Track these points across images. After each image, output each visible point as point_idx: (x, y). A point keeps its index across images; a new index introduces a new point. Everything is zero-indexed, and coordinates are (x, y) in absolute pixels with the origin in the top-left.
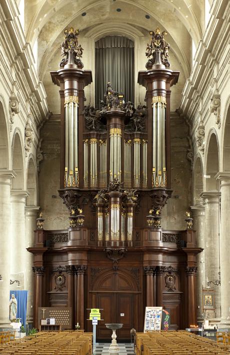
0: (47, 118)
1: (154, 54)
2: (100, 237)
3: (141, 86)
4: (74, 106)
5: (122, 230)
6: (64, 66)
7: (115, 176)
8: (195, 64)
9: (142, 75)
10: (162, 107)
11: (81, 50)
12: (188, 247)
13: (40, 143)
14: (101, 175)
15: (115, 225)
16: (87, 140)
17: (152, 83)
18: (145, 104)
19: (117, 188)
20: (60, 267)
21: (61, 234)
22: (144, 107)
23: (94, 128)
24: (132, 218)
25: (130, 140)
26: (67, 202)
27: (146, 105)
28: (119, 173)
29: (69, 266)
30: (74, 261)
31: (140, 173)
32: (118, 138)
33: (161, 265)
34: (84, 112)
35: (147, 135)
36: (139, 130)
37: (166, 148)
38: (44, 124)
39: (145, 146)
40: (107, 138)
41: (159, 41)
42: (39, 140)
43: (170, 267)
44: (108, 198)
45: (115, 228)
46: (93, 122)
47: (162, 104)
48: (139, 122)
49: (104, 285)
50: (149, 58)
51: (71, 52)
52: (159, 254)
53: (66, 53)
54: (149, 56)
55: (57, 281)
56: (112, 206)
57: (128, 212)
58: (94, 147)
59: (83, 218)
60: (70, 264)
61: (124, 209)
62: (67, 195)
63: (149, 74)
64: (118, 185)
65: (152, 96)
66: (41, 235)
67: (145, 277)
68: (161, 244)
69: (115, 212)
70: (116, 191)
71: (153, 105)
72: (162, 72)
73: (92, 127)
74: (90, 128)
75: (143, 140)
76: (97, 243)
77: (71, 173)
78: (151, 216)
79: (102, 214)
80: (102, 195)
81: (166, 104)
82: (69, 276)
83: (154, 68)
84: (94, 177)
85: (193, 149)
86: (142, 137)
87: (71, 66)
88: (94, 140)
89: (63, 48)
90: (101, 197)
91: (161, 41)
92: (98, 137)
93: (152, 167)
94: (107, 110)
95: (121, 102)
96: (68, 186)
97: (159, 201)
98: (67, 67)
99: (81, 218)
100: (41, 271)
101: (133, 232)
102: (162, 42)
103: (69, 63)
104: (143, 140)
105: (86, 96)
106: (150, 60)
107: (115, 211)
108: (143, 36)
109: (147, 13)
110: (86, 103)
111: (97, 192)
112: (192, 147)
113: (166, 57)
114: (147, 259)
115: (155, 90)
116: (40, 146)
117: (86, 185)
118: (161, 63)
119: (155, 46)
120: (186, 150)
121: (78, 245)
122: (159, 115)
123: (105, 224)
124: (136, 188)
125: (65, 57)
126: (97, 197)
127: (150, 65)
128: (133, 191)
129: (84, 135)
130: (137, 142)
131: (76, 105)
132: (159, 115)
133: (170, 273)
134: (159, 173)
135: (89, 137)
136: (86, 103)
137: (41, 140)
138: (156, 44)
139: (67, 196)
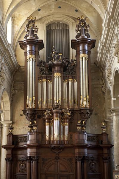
0: (17, 69)
1: (80, 30)
2: (47, 138)
3: (73, 49)
4: (32, 61)
5: (61, 133)
6: (27, 38)
10: (86, 60)
11: (37, 29)
12: (103, 144)
13: (13, 83)
14: (49, 101)
15: (56, 130)
16: (40, 80)
17: (79, 46)
18: (75, 58)
20: (23, 158)
21: (23, 137)
22: (75, 60)
23: (44, 73)
25: (67, 80)
26: (28, 118)
27: (76, 60)
28: (59, 99)
29: (28, 157)
32: (59, 78)
33: (86, 156)
34: (39, 64)
36: (72, 74)
37: (88, 84)
38: (16, 72)
39: (76, 83)
40: (52, 79)
41: (83, 23)
42: (12, 82)
43: (92, 157)
44: (52, 114)
45: (56, 133)
46: (44, 70)
47: (86, 58)
48: (72, 69)
49: (50, 169)
51: (31, 30)
52: (85, 149)
53: (28, 31)
55: (20, 167)
56: (55, 118)
58: (44, 84)
59: (36, 126)
60: (28, 155)
61: (62, 121)
62: (28, 113)
63: (77, 41)
64: (58, 106)
65: (79, 54)
66: (11, 137)
67: (76, 163)
68: (86, 142)
69: (57, 122)
71: (80, 59)
72: (85, 40)
75: (75, 80)
77: (31, 99)
78: (79, 124)
79: (48, 124)
81: (88, 58)
82: (28, 163)
84: (44, 102)
85: (105, 85)
86: (73, 78)
87: (31, 37)
88: (44, 80)
89: (26, 28)
90: (48, 113)
93: (80, 96)
96: (28, 107)
97: (85, 116)
98: (28, 38)
99: (35, 126)
100: (10, 160)
101: (68, 135)
102: (85, 24)
103: (30, 36)
104: (75, 80)
106: (78, 34)
107: (57, 122)
108: (74, 22)
109: (76, 8)
111: (45, 111)
112: (104, 84)
113: (87, 32)
114: (78, 152)
115: (81, 50)
116: (13, 85)
117: (40, 107)
118: (84, 35)
119: (81, 26)
120: (101, 87)
121: (34, 143)
122: (83, 65)
125: (28, 33)
126: (45, 113)
127: (78, 36)
129: (38, 79)
131: (34, 60)
132: (83, 65)
133: (92, 161)
134: (85, 99)
135: (42, 78)
136: (40, 59)
137: (14, 82)
138: (81, 24)
139: (28, 114)
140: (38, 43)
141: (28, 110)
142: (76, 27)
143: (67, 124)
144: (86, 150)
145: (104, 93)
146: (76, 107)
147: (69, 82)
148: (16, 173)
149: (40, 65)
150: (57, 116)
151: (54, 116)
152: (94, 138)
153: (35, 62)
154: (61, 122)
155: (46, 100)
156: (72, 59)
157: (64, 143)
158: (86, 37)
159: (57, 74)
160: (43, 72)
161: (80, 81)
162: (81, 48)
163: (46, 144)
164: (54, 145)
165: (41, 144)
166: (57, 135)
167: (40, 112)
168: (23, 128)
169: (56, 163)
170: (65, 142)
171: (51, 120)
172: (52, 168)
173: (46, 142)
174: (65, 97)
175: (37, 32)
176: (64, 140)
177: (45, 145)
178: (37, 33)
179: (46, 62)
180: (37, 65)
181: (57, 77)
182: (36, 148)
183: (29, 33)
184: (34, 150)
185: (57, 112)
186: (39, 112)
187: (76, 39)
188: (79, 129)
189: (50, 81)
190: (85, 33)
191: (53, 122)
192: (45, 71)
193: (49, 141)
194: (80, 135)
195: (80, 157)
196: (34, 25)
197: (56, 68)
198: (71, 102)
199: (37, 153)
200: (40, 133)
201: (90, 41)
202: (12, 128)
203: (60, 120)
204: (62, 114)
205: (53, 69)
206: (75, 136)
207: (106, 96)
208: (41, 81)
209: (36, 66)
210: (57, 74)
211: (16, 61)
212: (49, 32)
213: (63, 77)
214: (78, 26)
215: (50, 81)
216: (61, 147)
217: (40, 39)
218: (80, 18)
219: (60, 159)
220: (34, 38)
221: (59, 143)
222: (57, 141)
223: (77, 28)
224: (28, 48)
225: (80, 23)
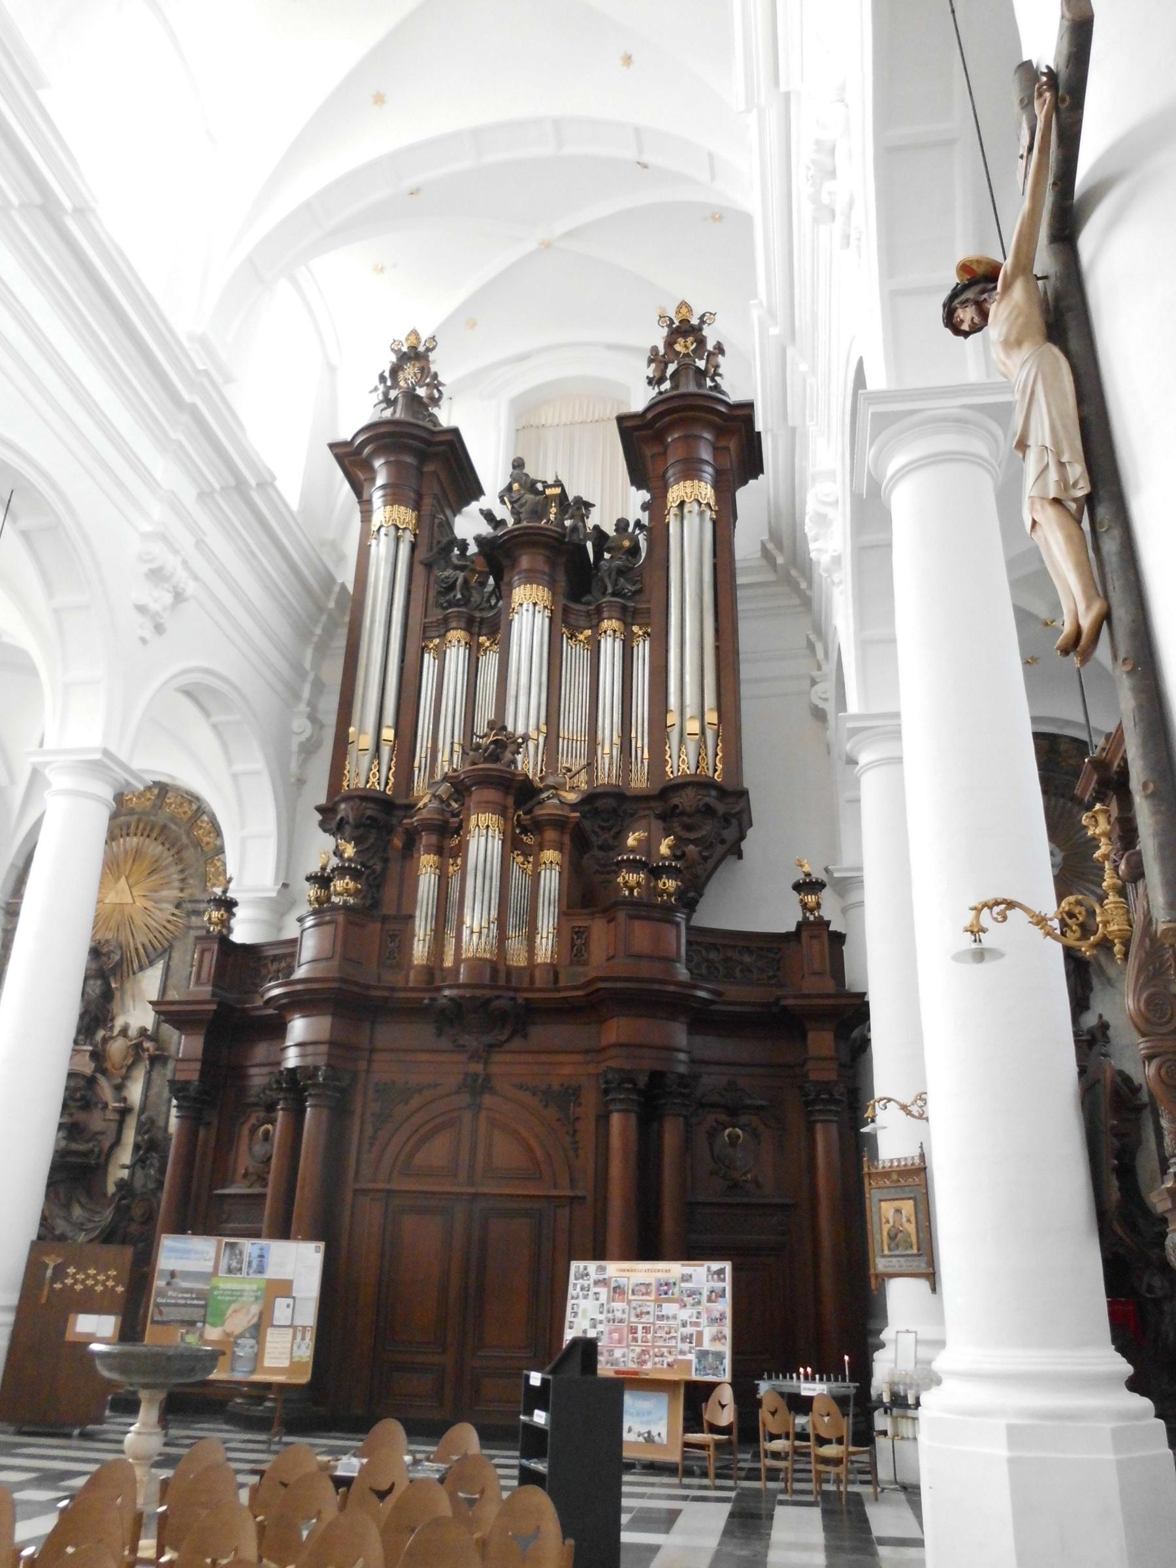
2: (420, 951)
18: (645, 518)
25: (588, 632)
33: (682, 1069)
35: (648, 610)
37: (717, 648)
39: (643, 650)
47: (700, 504)
49: (419, 1159)
58: (456, 657)
60: (292, 1059)
67: (603, 1119)
69: (484, 841)
75: (635, 629)
76: (408, 976)
86: (628, 616)
90: (439, 798)
92: (473, 626)
100: (184, 1098)
102: (701, 342)
104: (635, 629)
134: (693, 726)
135: (444, 626)
138: (678, 347)
147: (599, 641)
148: (223, 1187)
150: (485, 807)
152: (747, 959)
153: (414, 547)
154: (512, 844)
157: (526, 979)
166: (476, 929)
169: (467, 1117)
171: (448, 835)
172: (437, 1152)
173: (412, 974)
180: (421, 563)
181: (529, 614)
188: (631, 890)
191: (461, 850)
197: (525, 562)
201: (723, 409)
209: (419, 569)
211: (305, 543)
215: (488, 644)
218: (671, 319)
219: (492, 1090)
221: (487, 980)
222: (477, 963)
223: (653, 365)
225: (670, 344)
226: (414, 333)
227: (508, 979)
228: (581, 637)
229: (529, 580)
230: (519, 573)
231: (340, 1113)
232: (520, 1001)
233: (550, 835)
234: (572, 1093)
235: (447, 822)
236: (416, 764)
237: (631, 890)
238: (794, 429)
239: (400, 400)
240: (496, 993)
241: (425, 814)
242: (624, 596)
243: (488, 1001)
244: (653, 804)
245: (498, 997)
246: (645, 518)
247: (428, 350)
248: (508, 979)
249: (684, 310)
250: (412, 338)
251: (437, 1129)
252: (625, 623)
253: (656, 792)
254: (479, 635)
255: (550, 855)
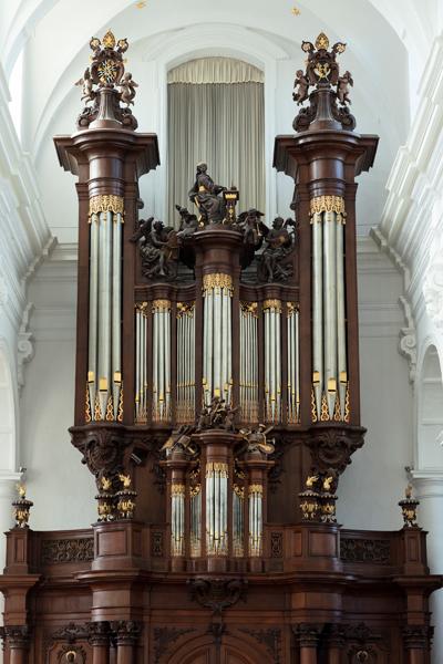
0: (46, 252)
1: (313, 97)
2: (177, 546)
4: (112, 221)
5: (234, 529)
6: (87, 125)
7: (217, 393)
8: (416, 119)
9: (283, 144)
10: (336, 222)
11: (132, 86)
12: (407, 573)
13: (26, 313)
14: (180, 392)
15: (214, 516)
16: (145, 304)
17: (309, 164)
18: (292, 215)
19: (220, 421)
20: (72, 626)
21: (76, 541)
22: (290, 222)
23: (162, 273)
24: (260, 499)
25: (255, 305)
26: (92, 460)
27: (294, 220)
28: (225, 386)
29: (96, 623)
30: (109, 611)
31: (282, 387)
32: (225, 298)
33: (338, 621)
34: (137, 232)
35: (298, 291)
36: (277, 278)
38: (36, 268)
39: (294, 320)
41: (326, 65)
42: (23, 307)
43: (361, 626)
44: (198, 446)
45: (216, 529)
46: (161, 259)
48: (278, 260)
50: (301, 107)
51: (107, 93)
52: (332, 592)
53: (94, 95)
54: (301, 102)
56: (209, 467)
57: (250, 483)
58: (162, 320)
59: (132, 498)
60: (98, 616)
61: (240, 476)
62: (93, 441)
63: (301, 142)
64: (224, 414)
65: (310, 196)
66: (23, 543)
68: (337, 566)
69: (216, 482)
70: (220, 433)
71: (312, 217)
72: (334, 138)
73: (159, 271)
74: (153, 274)
75: (289, 305)
76: (170, 562)
77: (104, 384)
78: (309, 493)
79: (180, 487)
80: (183, 439)
81: (345, 214)
83: (314, 127)
84: (161, 397)
85: (416, 326)
86: (284, 296)
87: (107, 123)
88: (162, 304)
89: (86, 83)
90: (181, 446)
91: (330, 67)
92: (172, 296)
93: (312, 371)
94: (196, 231)
95: (231, 211)
96: (94, 418)
97: (330, 456)
98: (94, 126)
99: (126, 497)
101: (263, 534)
102: (334, 69)
103: (101, 118)
104: (289, 305)
105: (142, 196)
106: (303, 111)
108: (285, 59)
110: (143, 215)
111: (167, 433)
112: (411, 323)
113: (343, 104)
114: (302, 605)
115: (317, 181)
116: (25, 321)
118: (330, 118)
119: (317, 77)
120: (397, 333)
121: (120, 568)
123: (190, 512)
124: (271, 424)
125: (92, 104)
126: (169, 444)
127: (304, 121)
128: (264, 430)
130: (272, 309)
131: (118, 218)
133: (362, 642)
134: (331, 385)
135: (151, 296)
136: (143, 215)
137: (29, 307)
138: (317, 72)
139: (91, 445)
140: (134, 148)
141: (93, 429)
142: (297, 82)
143: (257, 488)
144: (336, 600)
145: (407, 357)
146: (293, 419)
149: (143, 238)
150: (217, 458)
151: (205, 457)
152: (370, 548)
153: (123, 225)
154: (233, 481)
155: (168, 389)
156: (275, 216)
157: (245, 566)
158: (338, 127)
159: (218, 279)
160: (155, 268)
161: (312, 310)
162: (316, 169)
163: (174, 570)
164: (205, 577)
165: (151, 572)
166: (217, 537)
167: (142, 436)
168: (70, 501)
169: (213, 649)
170: (248, 565)
171: (191, 473)
173: (173, 563)
174: (247, 376)
175: (129, 99)
176: (247, 558)
177: (166, 574)
178: (131, 107)
179: (177, 229)
180: (131, 241)
181: (217, 294)
182: (131, 589)
183: (98, 105)
184: (122, 597)
185: (217, 441)
186: (137, 435)
187: (294, 133)
188: (310, 513)
189: (183, 309)
190: (333, 106)
191: (201, 481)
192: (165, 263)
193: (186, 558)
194: (315, 535)
195: (312, 627)
196: (119, 69)
197: (215, 254)
198: (273, 398)
199: (136, 610)
200: (142, 523)
201: (352, 141)
202: (25, 506)
203: (228, 473)
204: (238, 448)
205: (198, 256)
206: (292, 542)
207: (417, 372)
208: (146, 308)
209: (129, 246)
210: (218, 279)
211: (42, 221)
212: (180, 96)
213: (242, 290)
214: (303, 80)
215: (183, 309)
216: (232, 585)
217: (142, 129)
218: (311, 45)
219: (228, 634)
220: (118, 127)
221: (224, 570)
222: (217, 559)
223: (298, 86)
224: (95, 168)
225: (311, 68)
226: (110, 35)
227: (236, 569)
228: (251, 309)
229: (217, 270)
230: (210, 264)
231: (136, 647)
232: (246, 582)
233: (258, 475)
234: (271, 637)
235: (189, 464)
236: (137, 398)
237: (310, 513)
238: (412, 201)
239: (103, 97)
240: (231, 577)
241: (174, 459)
242: (281, 280)
243: (227, 583)
244: (305, 436)
245: (234, 580)
246: (292, 215)
247: (122, 50)
248: (236, 569)
249: (322, 41)
250: (109, 40)
251: (195, 656)
252: (282, 301)
253: (306, 429)
254: (177, 302)
255: (257, 488)
